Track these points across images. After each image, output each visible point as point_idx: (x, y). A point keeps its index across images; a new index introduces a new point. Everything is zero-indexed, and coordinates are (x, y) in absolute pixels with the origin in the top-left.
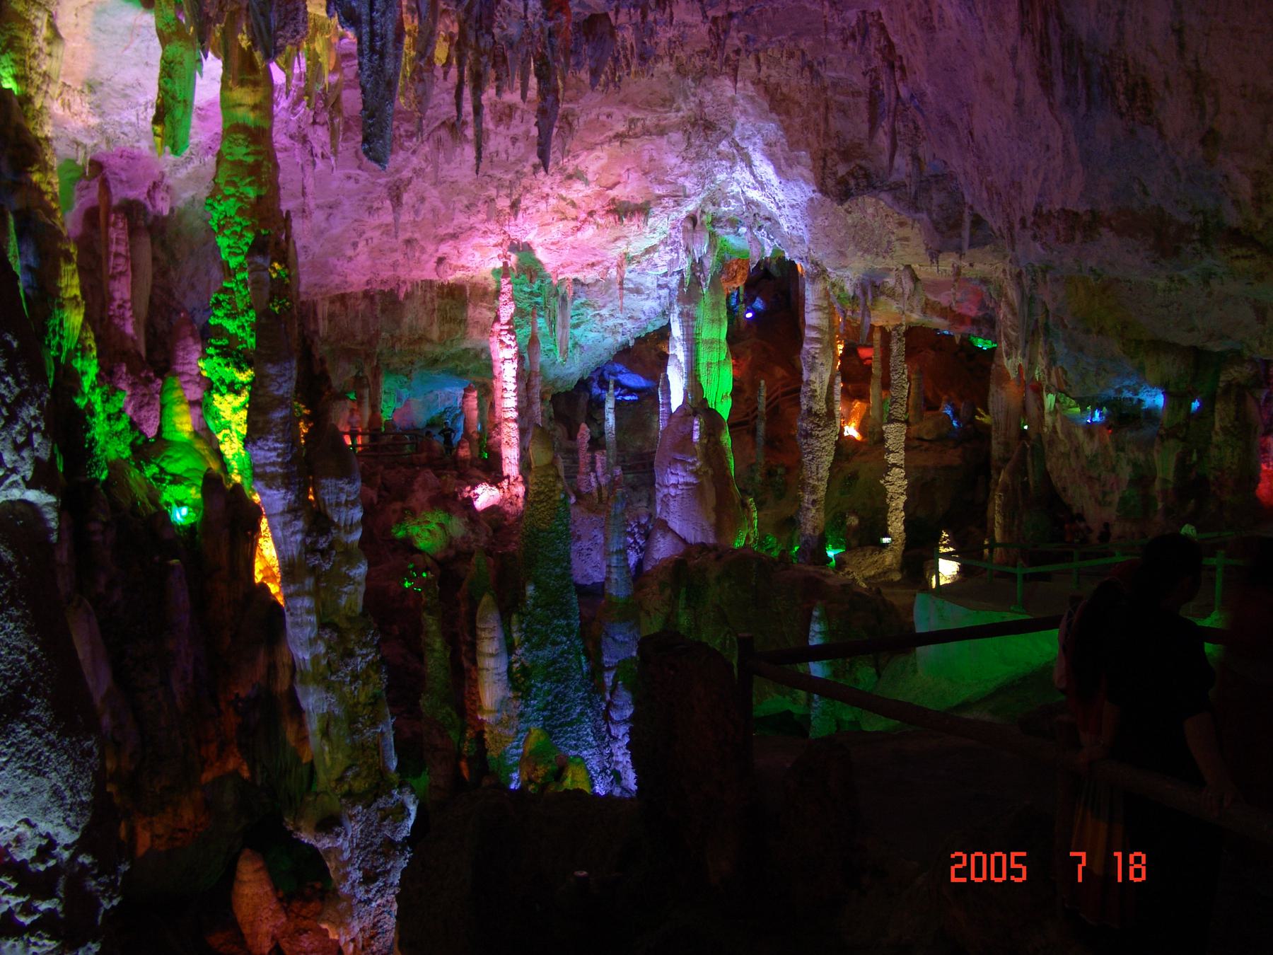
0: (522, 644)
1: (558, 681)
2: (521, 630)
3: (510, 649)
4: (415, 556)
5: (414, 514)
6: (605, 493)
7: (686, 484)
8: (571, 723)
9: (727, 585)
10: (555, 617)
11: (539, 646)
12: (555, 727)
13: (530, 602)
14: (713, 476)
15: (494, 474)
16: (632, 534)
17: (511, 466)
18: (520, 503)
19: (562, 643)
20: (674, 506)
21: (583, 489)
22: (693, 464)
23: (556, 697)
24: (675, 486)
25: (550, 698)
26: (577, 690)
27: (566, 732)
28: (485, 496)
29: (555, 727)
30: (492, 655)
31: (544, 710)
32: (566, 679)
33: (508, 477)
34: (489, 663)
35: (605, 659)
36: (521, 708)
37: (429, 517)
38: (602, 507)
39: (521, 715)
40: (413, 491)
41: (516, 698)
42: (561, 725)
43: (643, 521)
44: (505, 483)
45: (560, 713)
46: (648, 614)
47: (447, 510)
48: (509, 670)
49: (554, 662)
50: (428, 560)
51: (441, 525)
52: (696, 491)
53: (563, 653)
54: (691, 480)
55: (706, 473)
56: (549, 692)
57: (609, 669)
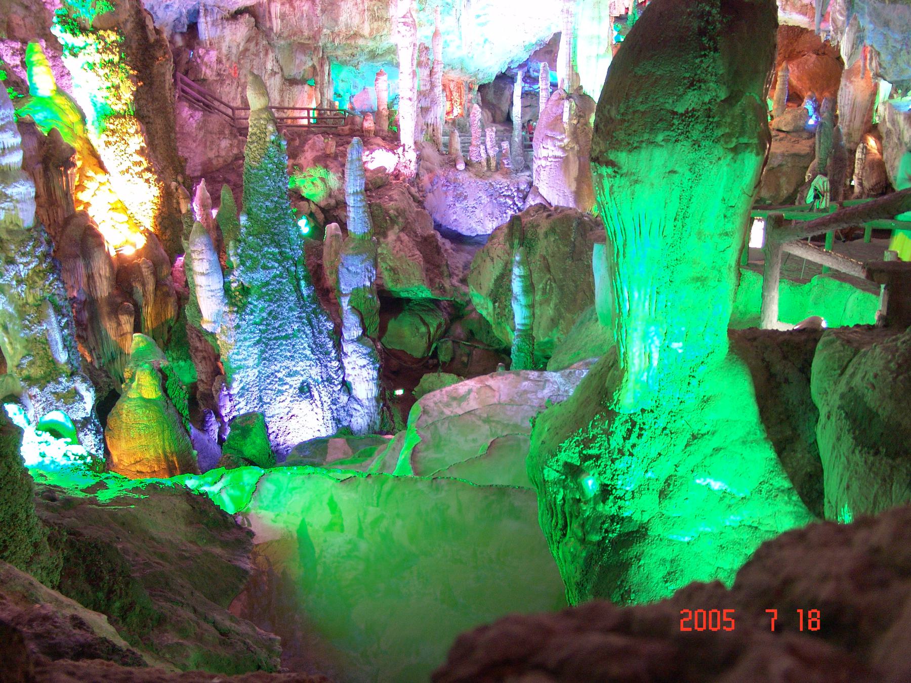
0: (238, 267)
1: (271, 301)
2: (237, 255)
3: (226, 271)
4: (302, 203)
5: (301, 169)
6: (493, 164)
7: (555, 157)
8: (287, 337)
9: (552, 239)
10: (266, 245)
11: (252, 269)
12: (270, 340)
13: (243, 230)
14: (579, 152)
15: (392, 140)
16: (511, 197)
17: (407, 136)
18: (413, 167)
19: (273, 268)
20: (544, 175)
21: (473, 159)
22: (561, 140)
23: (270, 314)
24: (546, 158)
25: (265, 315)
27: (281, 344)
29: (270, 340)
30: (203, 274)
31: (261, 324)
32: (278, 300)
33: (404, 145)
34: (200, 280)
35: (343, 287)
36: (237, 321)
37: (312, 172)
38: (489, 174)
39: (238, 327)
40: (304, 151)
41: (232, 312)
42: (275, 339)
43: (523, 187)
44: (400, 150)
45: (274, 328)
46: (492, 260)
47: (326, 167)
48: (227, 290)
49: (267, 284)
50: (313, 207)
52: (564, 163)
53: (275, 277)
54: (560, 153)
55: (572, 148)
56: (262, 310)
57: (346, 295)
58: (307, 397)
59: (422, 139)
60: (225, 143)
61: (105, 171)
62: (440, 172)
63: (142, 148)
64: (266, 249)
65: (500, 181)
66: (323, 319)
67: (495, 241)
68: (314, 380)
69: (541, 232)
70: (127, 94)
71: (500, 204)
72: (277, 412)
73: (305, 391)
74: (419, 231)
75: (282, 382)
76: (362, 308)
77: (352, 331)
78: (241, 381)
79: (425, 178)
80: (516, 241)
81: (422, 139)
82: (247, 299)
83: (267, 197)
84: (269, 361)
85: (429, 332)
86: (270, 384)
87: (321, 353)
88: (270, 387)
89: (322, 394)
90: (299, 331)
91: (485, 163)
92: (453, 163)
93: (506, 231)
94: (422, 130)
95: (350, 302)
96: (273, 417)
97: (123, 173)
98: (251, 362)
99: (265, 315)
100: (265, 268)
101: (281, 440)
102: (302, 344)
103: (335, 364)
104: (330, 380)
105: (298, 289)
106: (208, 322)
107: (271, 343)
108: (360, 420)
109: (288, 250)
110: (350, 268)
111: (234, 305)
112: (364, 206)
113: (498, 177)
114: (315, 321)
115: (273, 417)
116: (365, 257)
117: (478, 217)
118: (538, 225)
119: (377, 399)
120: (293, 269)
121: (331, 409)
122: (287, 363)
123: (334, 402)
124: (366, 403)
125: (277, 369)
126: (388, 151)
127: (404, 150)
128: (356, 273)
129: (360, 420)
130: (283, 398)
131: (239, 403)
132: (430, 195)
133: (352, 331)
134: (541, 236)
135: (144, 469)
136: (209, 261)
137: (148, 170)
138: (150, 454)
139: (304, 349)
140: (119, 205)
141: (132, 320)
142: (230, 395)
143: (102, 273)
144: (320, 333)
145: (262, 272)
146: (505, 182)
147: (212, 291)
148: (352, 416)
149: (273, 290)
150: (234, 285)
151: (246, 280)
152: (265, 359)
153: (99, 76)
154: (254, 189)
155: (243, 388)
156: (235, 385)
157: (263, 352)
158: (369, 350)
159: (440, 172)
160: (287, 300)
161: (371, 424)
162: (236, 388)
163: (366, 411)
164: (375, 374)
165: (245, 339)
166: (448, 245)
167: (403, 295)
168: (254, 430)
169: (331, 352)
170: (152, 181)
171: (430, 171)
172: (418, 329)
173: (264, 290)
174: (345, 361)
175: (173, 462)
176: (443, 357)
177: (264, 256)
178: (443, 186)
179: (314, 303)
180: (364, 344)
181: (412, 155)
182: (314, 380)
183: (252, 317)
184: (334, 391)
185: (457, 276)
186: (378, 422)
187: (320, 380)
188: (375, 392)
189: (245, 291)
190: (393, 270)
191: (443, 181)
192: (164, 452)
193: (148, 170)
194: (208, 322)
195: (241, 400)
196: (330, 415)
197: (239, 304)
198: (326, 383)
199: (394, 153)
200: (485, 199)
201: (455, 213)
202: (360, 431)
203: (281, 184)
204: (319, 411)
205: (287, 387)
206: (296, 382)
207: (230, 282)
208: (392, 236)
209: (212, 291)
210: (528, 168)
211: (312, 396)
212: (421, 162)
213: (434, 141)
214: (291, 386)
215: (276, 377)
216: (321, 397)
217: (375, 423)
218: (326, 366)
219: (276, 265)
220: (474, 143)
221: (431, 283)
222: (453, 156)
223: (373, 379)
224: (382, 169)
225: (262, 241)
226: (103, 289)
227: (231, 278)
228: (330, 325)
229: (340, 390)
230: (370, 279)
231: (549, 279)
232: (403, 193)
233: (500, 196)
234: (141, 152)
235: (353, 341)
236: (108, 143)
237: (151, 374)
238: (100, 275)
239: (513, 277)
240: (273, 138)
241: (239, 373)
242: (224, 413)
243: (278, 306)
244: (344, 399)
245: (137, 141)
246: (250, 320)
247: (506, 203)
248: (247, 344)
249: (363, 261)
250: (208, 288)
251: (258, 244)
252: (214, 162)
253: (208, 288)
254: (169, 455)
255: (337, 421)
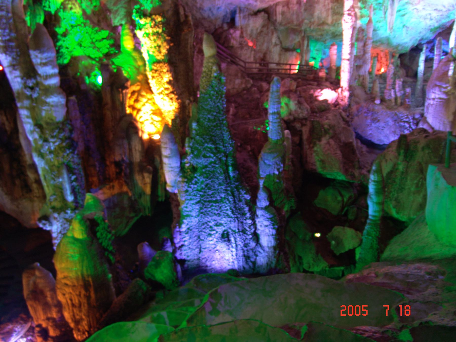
1: (207, 178)
2: (189, 146)
3: (182, 155)
6: (399, 101)
8: (217, 202)
9: (427, 152)
11: (197, 157)
12: (205, 201)
13: (194, 132)
15: (335, 84)
16: (408, 123)
18: (346, 100)
23: (206, 185)
25: (203, 186)
26: (220, 184)
28: (327, 95)
29: (205, 201)
30: (166, 157)
32: (212, 178)
34: (165, 160)
35: (261, 173)
36: (186, 187)
38: (395, 107)
39: (187, 191)
43: (417, 116)
44: (340, 90)
45: (208, 195)
46: (386, 161)
47: (289, 97)
49: (206, 167)
51: (286, 104)
53: (211, 163)
56: (202, 183)
57: (262, 178)
58: (225, 241)
59: (356, 84)
60: (238, 81)
61: (152, 92)
62: (364, 104)
63: (170, 81)
64: (206, 145)
65: (402, 112)
66: (243, 192)
67: (390, 149)
68: (232, 230)
69: (420, 146)
70: (164, 51)
71: (401, 126)
72: (208, 246)
73: (225, 237)
74: (343, 139)
75: (212, 229)
76: (271, 188)
77: (263, 201)
78: (188, 224)
79: (354, 108)
80: (402, 151)
81: (356, 84)
82: (194, 174)
83: (209, 112)
84: (204, 214)
85: (343, 201)
86: (204, 228)
87: (239, 214)
88: (204, 230)
89: (237, 240)
90: (225, 198)
91: (393, 101)
92: (373, 99)
93: (397, 143)
94: (355, 79)
95: (264, 183)
96: (205, 248)
97: (159, 94)
98: (194, 214)
99: (203, 186)
100: (205, 157)
101: (208, 264)
102: (226, 207)
103: (249, 222)
104: (244, 231)
105: (226, 172)
106: (169, 186)
107: (206, 204)
108: (262, 259)
109: (221, 147)
110: (266, 161)
111: (185, 177)
112: (279, 122)
113: (401, 110)
114: (236, 193)
115: (205, 248)
116: (275, 155)
117: (385, 133)
118: (418, 142)
119: (275, 248)
120: (224, 159)
121: (243, 249)
122: (215, 217)
123: (246, 245)
124: (267, 249)
125: (209, 220)
126: (332, 90)
127: (342, 90)
128: (269, 165)
129: (262, 259)
130: (211, 238)
131: (185, 237)
132: (356, 118)
133: (263, 201)
134: (420, 149)
135: (68, 282)
136: (171, 149)
137: (172, 92)
138: (72, 275)
139: (227, 210)
140: (158, 112)
141: (151, 176)
142: (180, 232)
143: (137, 148)
144: (240, 201)
145: (203, 159)
146: (405, 113)
147: (172, 167)
148: (257, 256)
149: (209, 171)
150: (187, 165)
151: (194, 162)
152: (202, 213)
153: (150, 40)
154: (202, 107)
155: (188, 229)
156: (183, 226)
157: (201, 209)
158: (271, 216)
159: (364, 104)
160: (218, 178)
161: (269, 263)
162: (184, 228)
163: (266, 254)
164: (274, 232)
165: (191, 199)
166: (365, 149)
167: (329, 176)
168: (163, 264)
169: (246, 214)
170: (174, 99)
171: (357, 103)
172: (336, 198)
173: (204, 170)
174: (257, 220)
175: (88, 281)
176: (351, 217)
177: (204, 149)
178: (365, 112)
179: (237, 182)
180: (269, 212)
181: (346, 94)
182: (232, 230)
183: (196, 186)
184: (246, 238)
185: (367, 168)
186: (274, 262)
187: (237, 231)
188: (273, 243)
189: (194, 169)
190: (322, 161)
191: (365, 110)
192: (82, 275)
193: (172, 92)
194: (169, 186)
195: (186, 235)
196: (242, 253)
197: (189, 177)
198: (241, 233)
199: (336, 92)
200: (391, 123)
201: (371, 130)
202: (262, 266)
203: (219, 104)
204: (234, 250)
205: (215, 232)
206: (220, 230)
207: (185, 163)
208: (324, 141)
209: (172, 167)
210: (423, 105)
211: (229, 240)
212: (353, 98)
213: (363, 86)
214: (217, 232)
215: (208, 225)
216: (236, 241)
217: (272, 263)
218: (242, 223)
219: (212, 155)
220: (388, 88)
221: (346, 172)
222: (374, 96)
223: (272, 235)
224: (326, 101)
225: (204, 139)
226: (137, 157)
227: (186, 161)
228: (248, 197)
229: (251, 238)
230: (278, 170)
231: (422, 178)
232: (335, 115)
233: (401, 121)
234: (169, 83)
235: (262, 209)
236: (153, 77)
237: (80, 222)
238: (136, 150)
239: (370, 181)
240: (215, 75)
241: (186, 219)
242: (176, 241)
243: (212, 182)
244: (253, 244)
245: (167, 77)
246: (194, 188)
247: (404, 126)
248: (192, 202)
249: (274, 158)
250: (169, 166)
251: (202, 141)
252: (231, 91)
253: (169, 166)
254: (86, 276)
255: (247, 258)
